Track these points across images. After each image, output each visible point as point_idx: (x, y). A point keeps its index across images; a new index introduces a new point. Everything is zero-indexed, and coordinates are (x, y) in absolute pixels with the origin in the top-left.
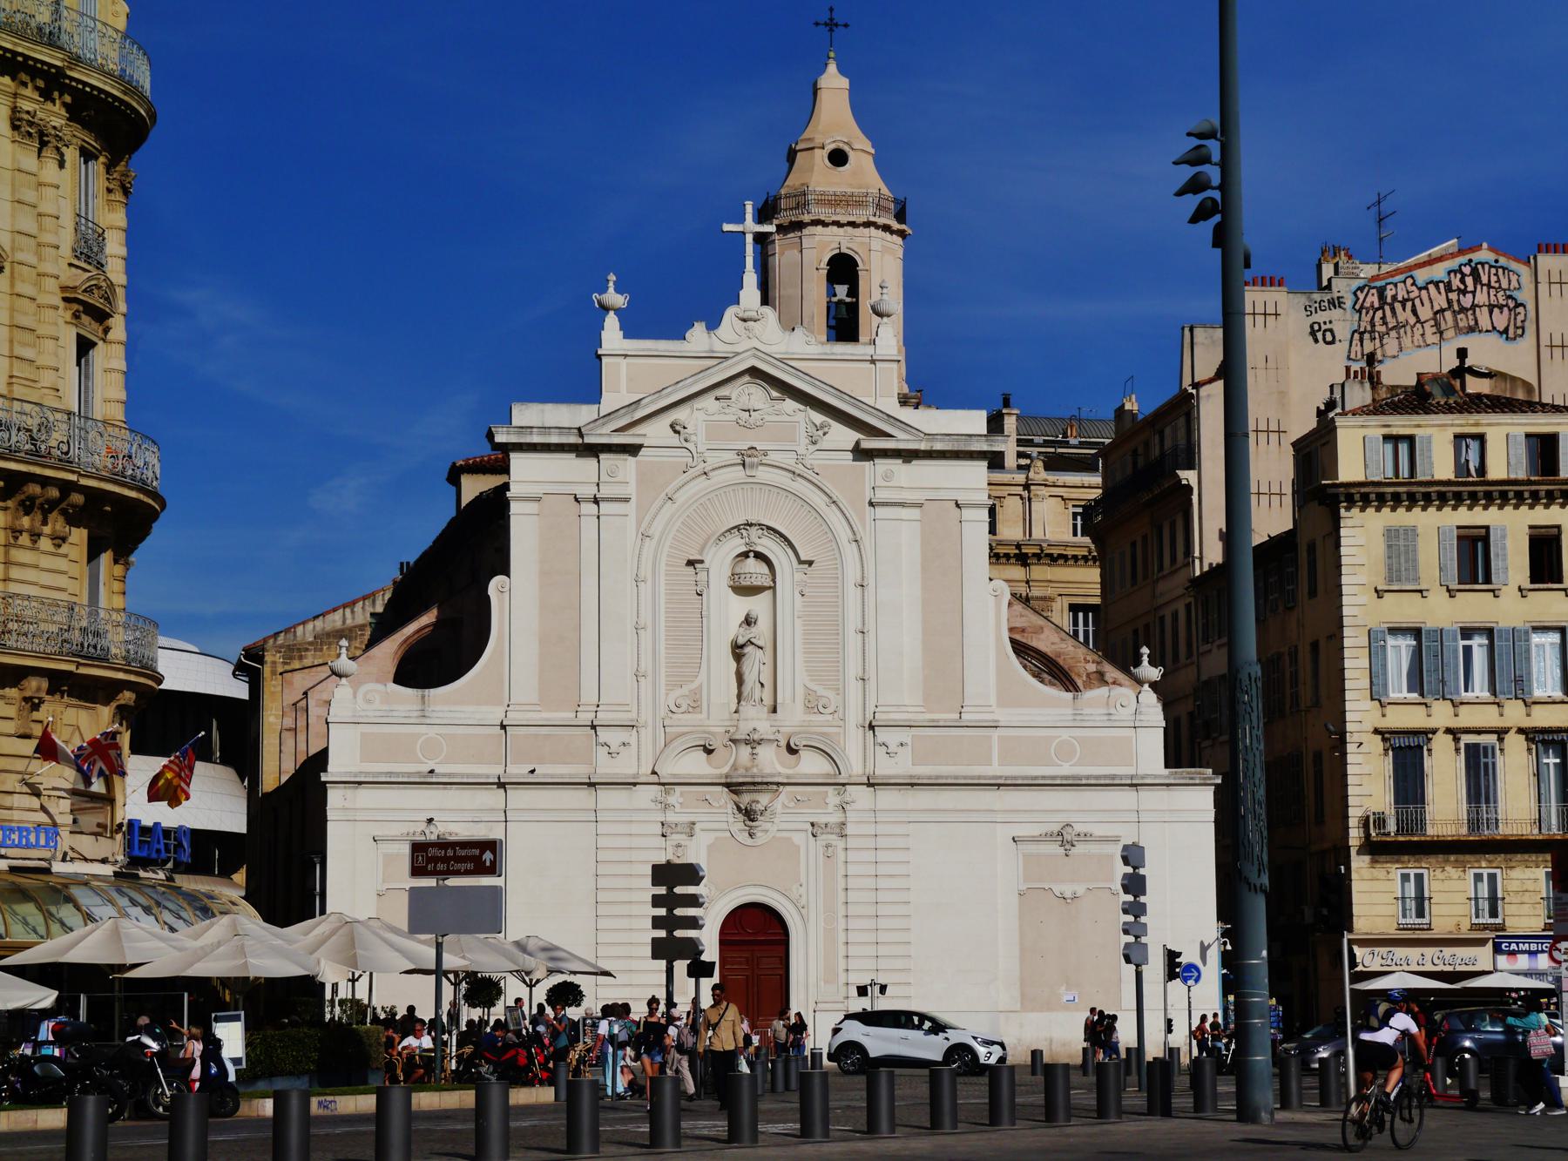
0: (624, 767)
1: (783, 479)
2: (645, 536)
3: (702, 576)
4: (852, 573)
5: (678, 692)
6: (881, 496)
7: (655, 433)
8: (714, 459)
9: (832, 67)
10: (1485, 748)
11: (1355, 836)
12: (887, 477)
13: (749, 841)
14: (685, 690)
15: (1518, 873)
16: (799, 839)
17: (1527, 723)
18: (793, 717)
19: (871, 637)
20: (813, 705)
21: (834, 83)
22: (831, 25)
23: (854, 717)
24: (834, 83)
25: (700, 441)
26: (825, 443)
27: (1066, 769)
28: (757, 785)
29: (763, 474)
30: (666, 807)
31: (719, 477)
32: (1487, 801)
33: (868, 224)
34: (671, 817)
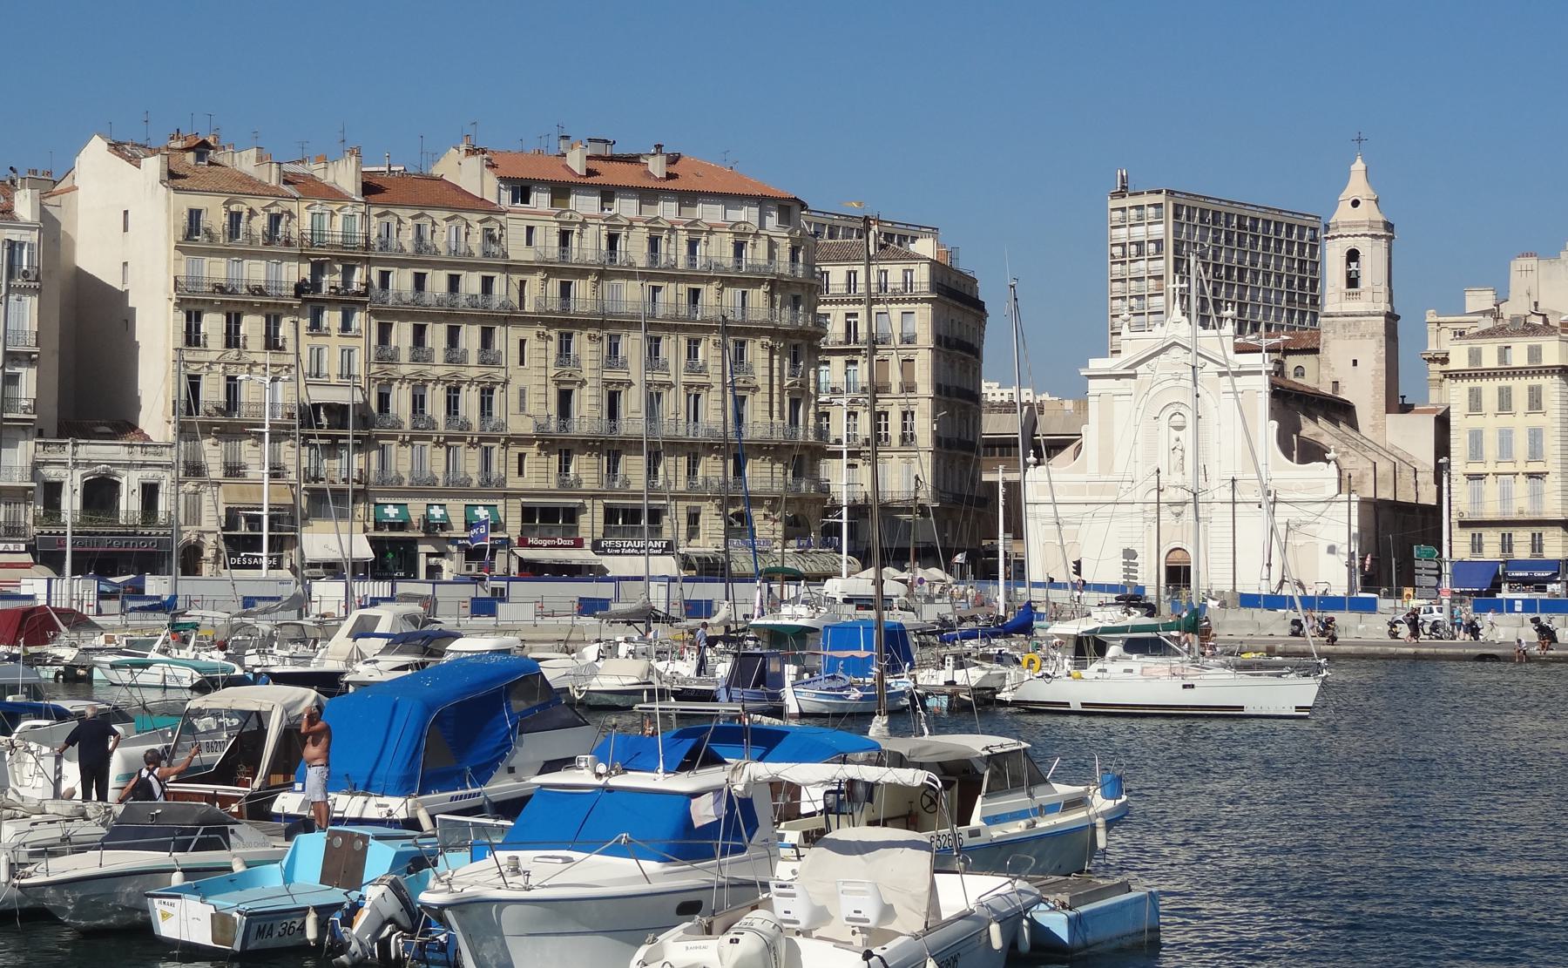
0: (1128, 498)
8: (1163, 378)
9: (1359, 160)
21: (1359, 166)
22: (1359, 140)
24: (1359, 166)
31: (1165, 385)
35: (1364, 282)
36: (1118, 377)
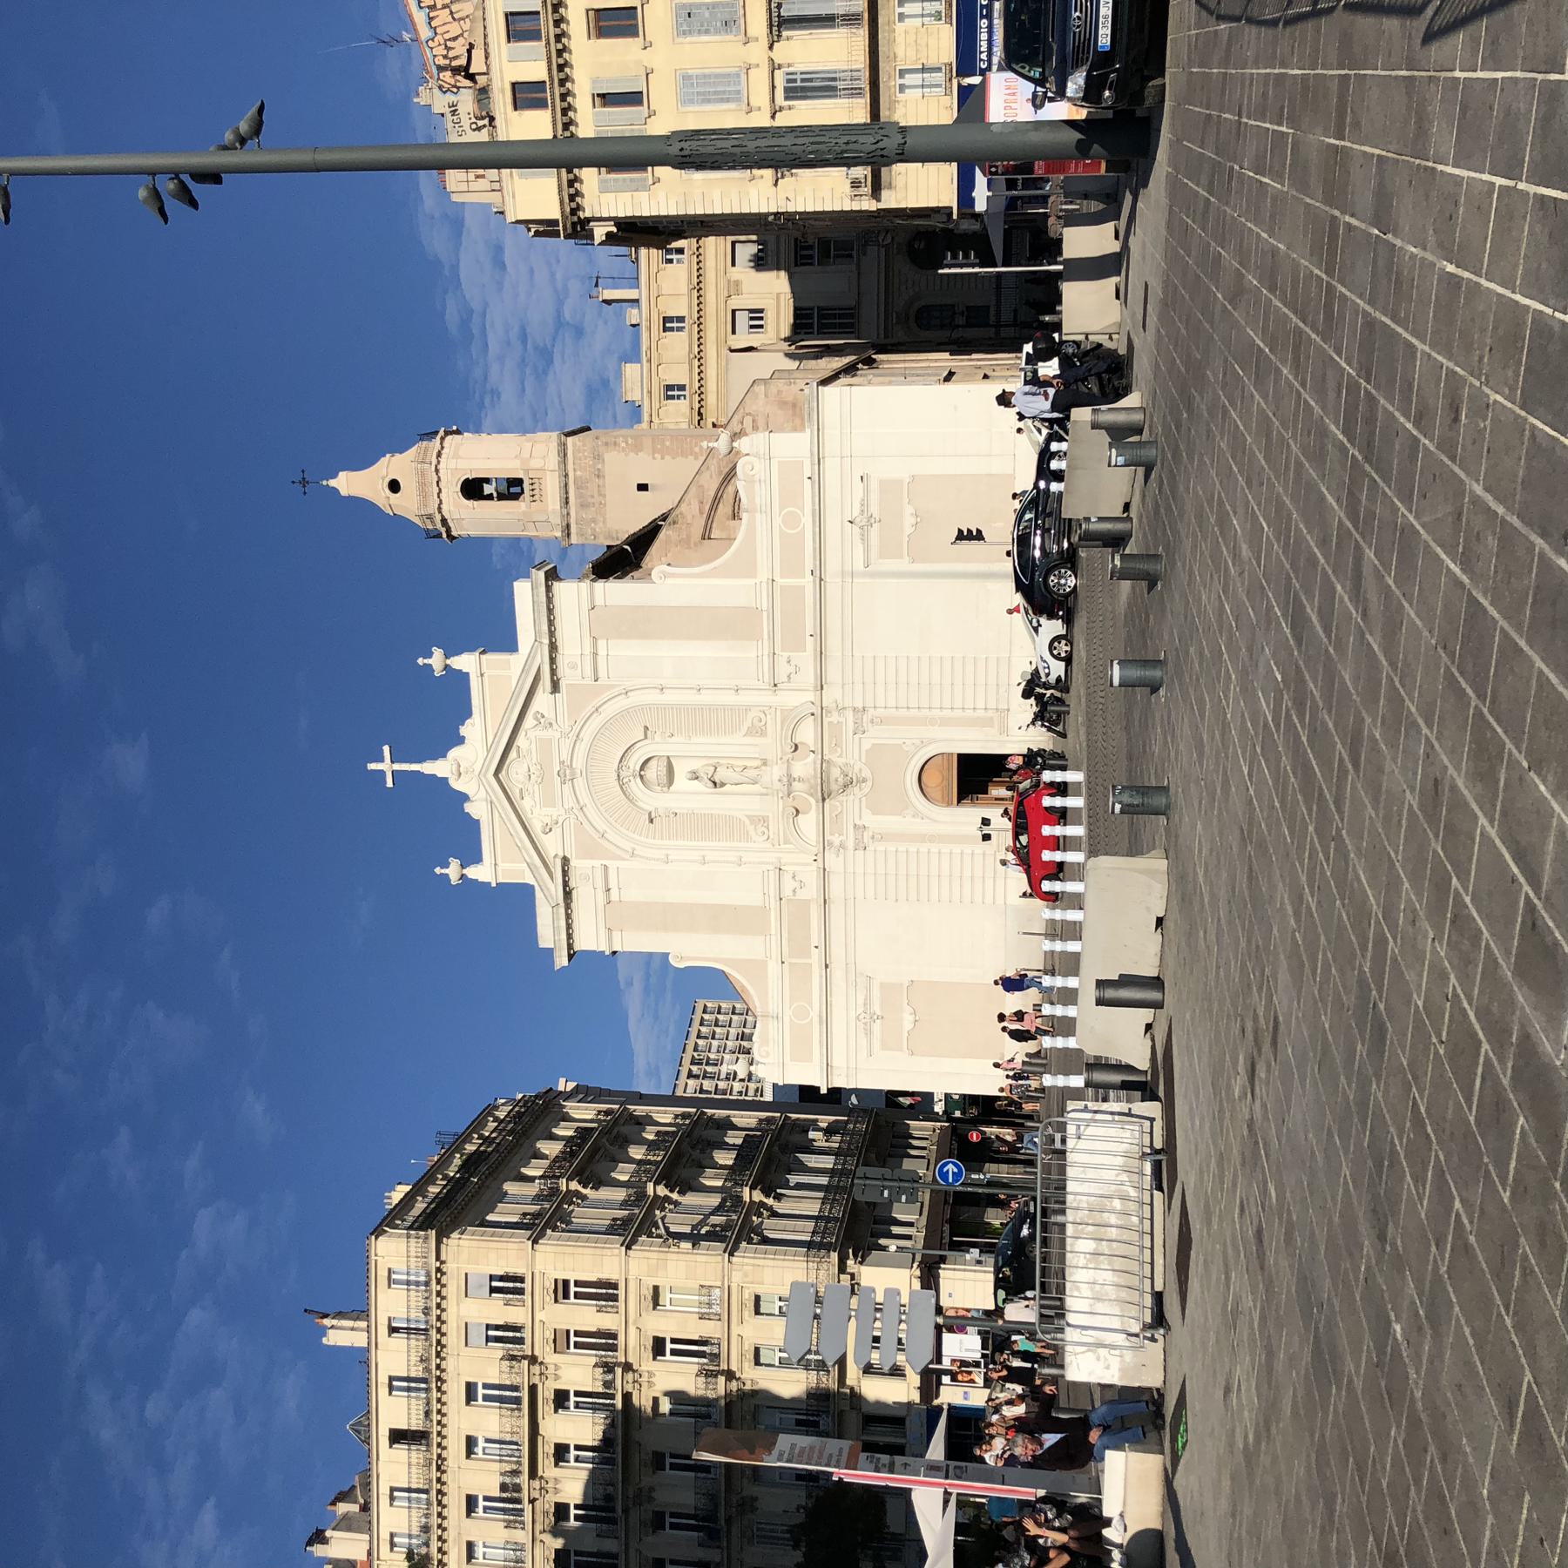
1: (582, 748)
3: (661, 812)
4: (652, 697)
5: (752, 833)
6: (589, 671)
7: (553, 847)
8: (570, 802)
9: (332, 483)
10: (789, 81)
11: (868, 205)
12: (574, 667)
13: (869, 783)
14: (751, 828)
15: (900, 51)
16: (866, 745)
17: (764, 42)
18: (772, 745)
20: (758, 731)
21: (346, 483)
22: (304, 482)
23: (768, 698)
24: (346, 483)
25: (555, 812)
26: (550, 715)
27: (807, 521)
29: (579, 763)
30: (842, 846)
32: (834, 79)
33: (437, 471)
34: (850, 844)
35: (512, 469)
36: (568, 894)
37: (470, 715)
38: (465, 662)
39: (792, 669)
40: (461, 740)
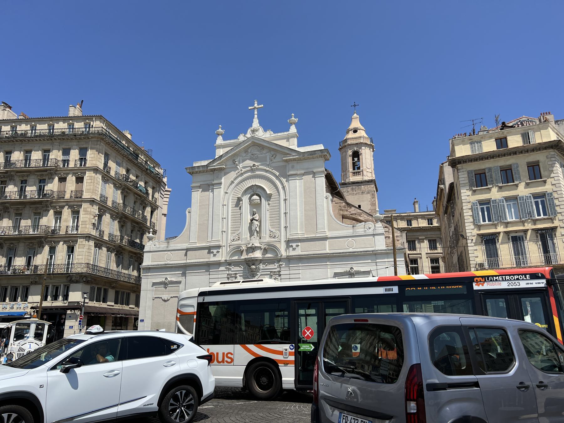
2: (227, 193)
10: (519, 237)
19: (288, 215)
22: (355, 106)
23: (283, 239)
28: (254, 261)
32: (522, 255)
37: (274, 133)
38: (293, 130)
39: (294, 247)
40: (265, 130)
